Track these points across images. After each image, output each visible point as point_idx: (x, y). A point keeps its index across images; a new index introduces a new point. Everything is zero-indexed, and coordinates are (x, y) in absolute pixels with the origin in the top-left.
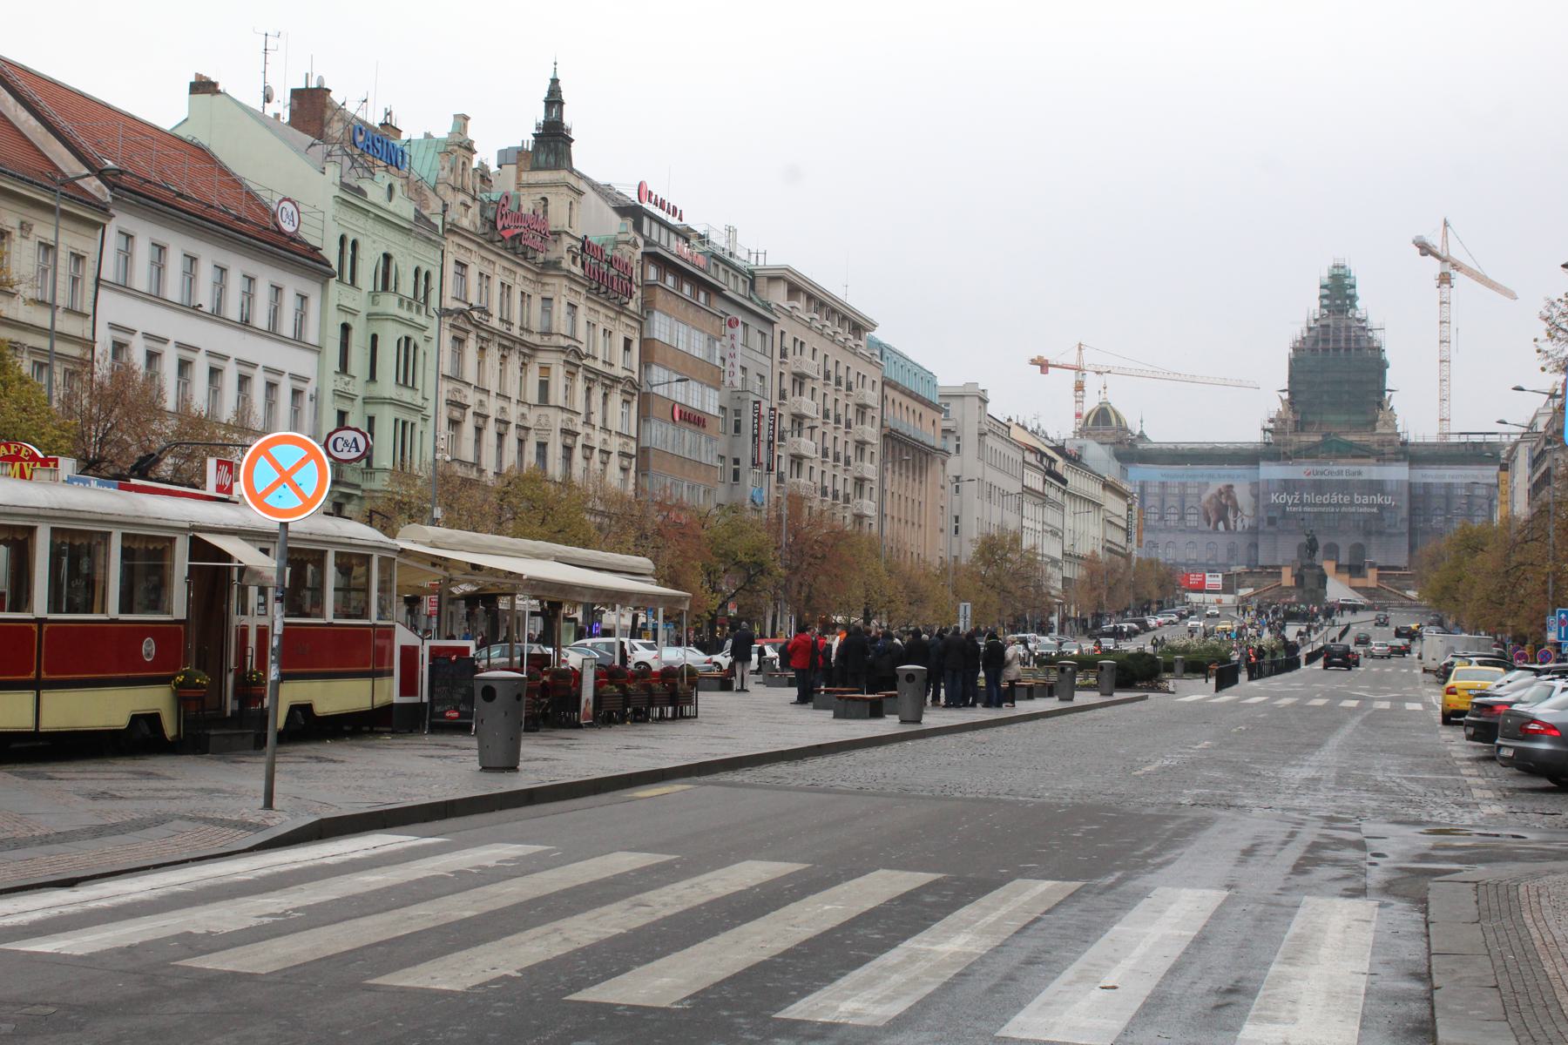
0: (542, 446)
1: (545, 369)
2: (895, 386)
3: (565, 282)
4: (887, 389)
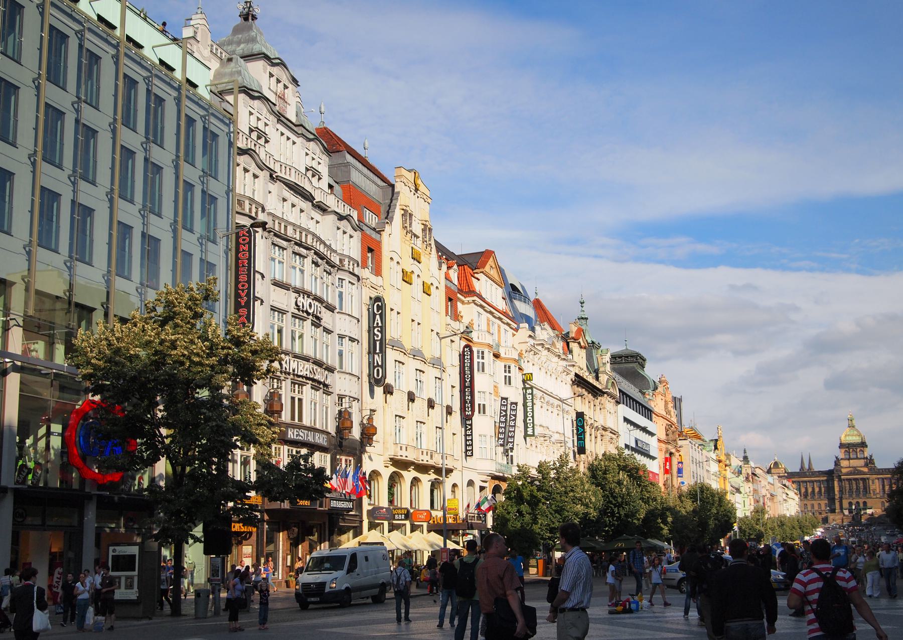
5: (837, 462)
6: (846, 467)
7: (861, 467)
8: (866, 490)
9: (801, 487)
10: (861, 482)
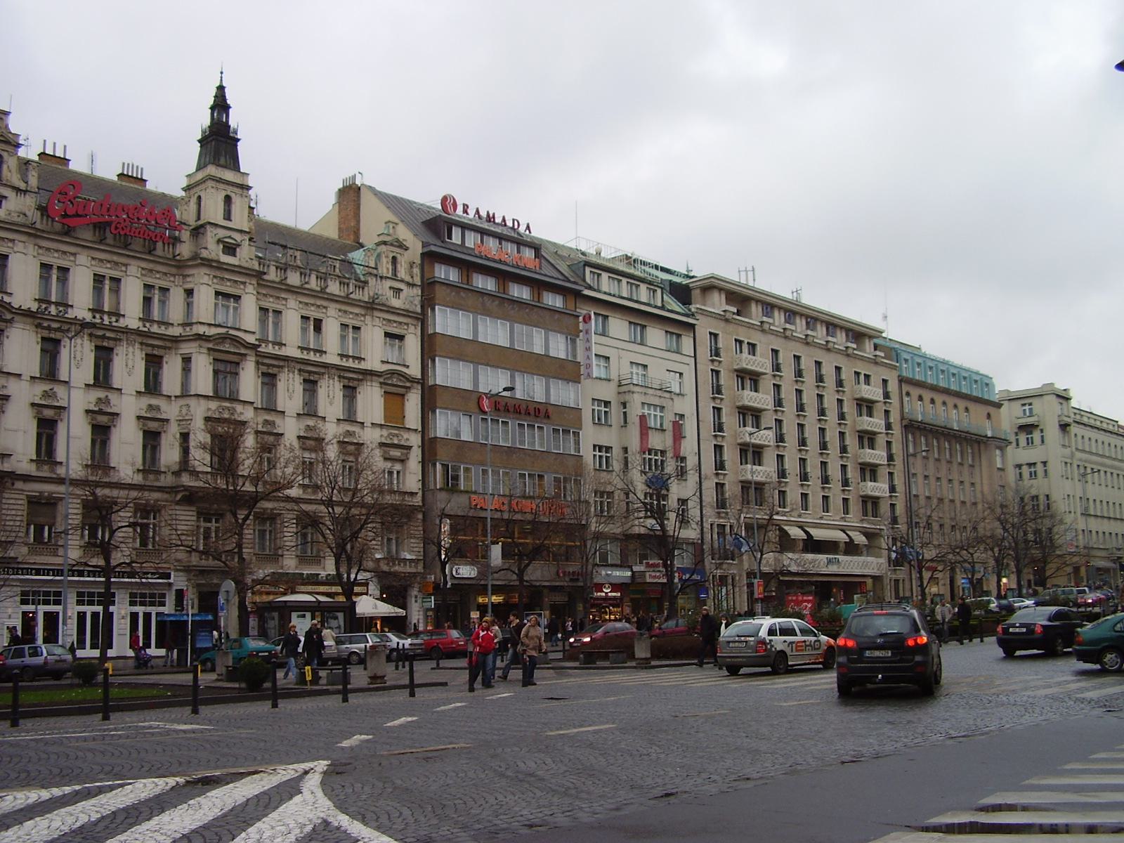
0: (185, 437)
1: (187, 360)
3: (204, 270)
4: (905, 388)
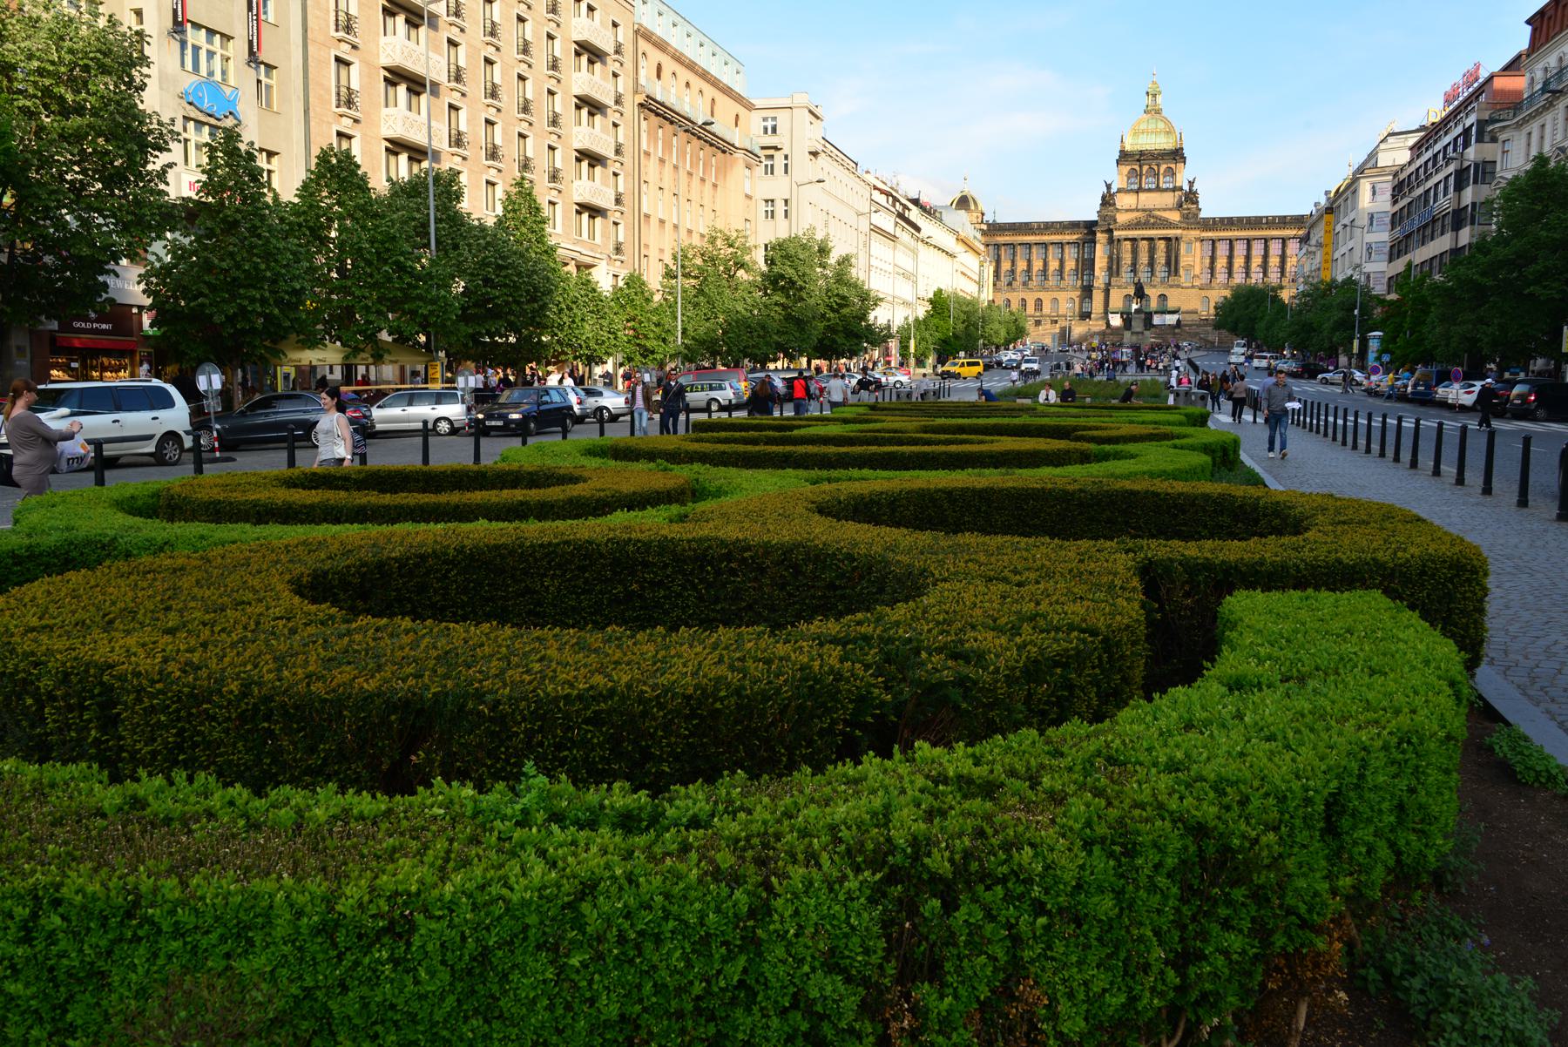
2: (661, 46)
4: (643, 45)
5: (1107, 201)
6: (1127, 211)
7: (1165, 210)
8: (1173, 265)
9: (1018, 258)
10: (1161, 245)
